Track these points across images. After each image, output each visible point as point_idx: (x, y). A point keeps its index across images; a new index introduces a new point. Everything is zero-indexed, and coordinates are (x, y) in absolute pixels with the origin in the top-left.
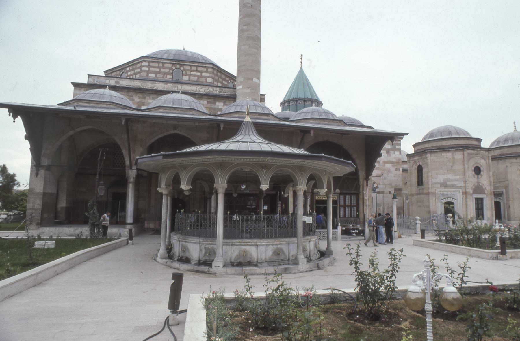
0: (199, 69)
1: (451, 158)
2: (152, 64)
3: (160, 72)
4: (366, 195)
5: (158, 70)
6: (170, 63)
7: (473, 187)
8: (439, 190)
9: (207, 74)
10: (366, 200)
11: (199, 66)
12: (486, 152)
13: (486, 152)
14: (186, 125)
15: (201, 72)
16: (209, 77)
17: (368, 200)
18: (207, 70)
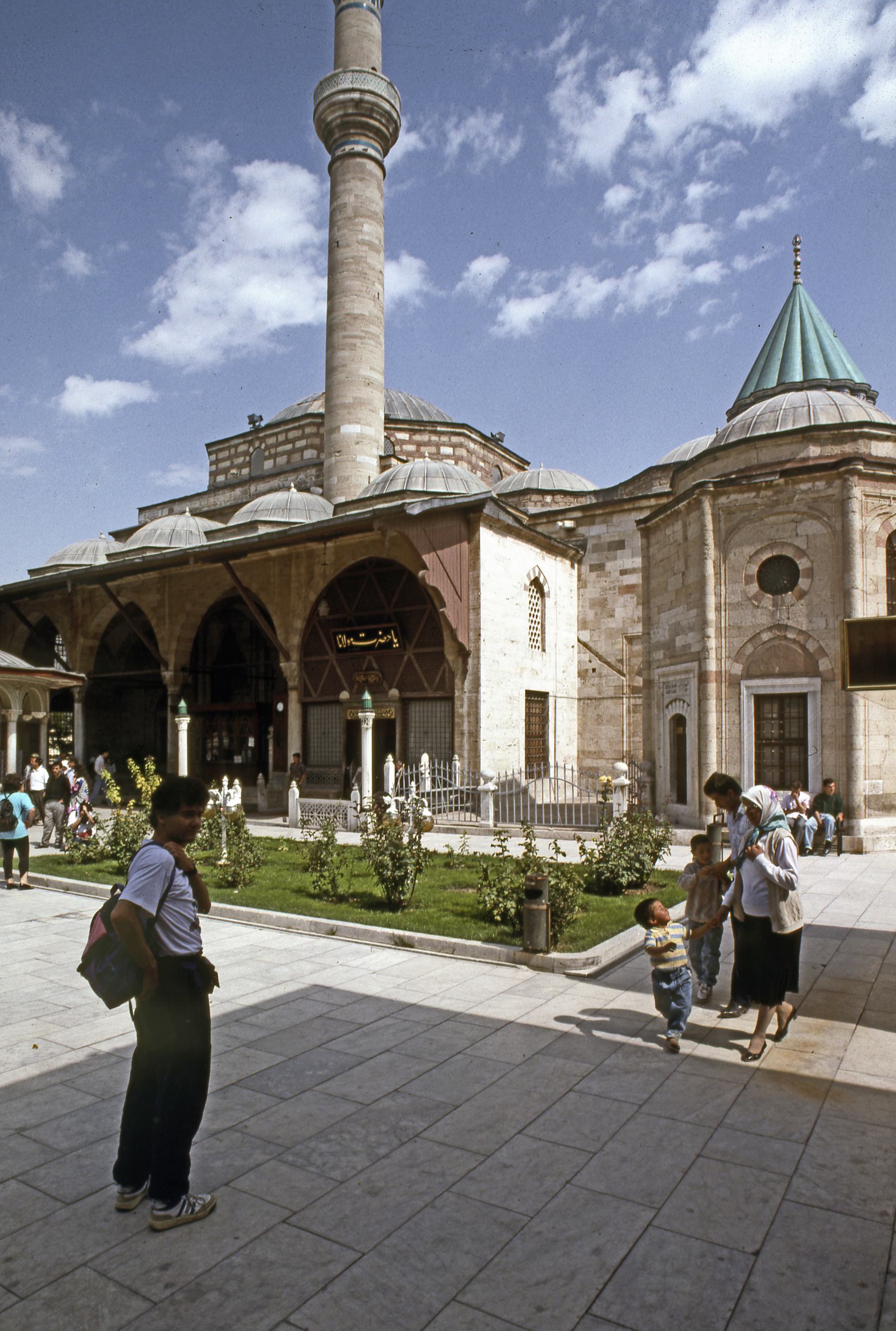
0: (291, 435)
1: (682, 542)
2: (221, 455)
3: (232, 466)
4: (462, 700)
5: (227, 464)
6: (244, 443)
7: (750, 649)
8: (660, 671)
9: (301, 443)
10: (462, 716)
11: (290, 430)
12: (829, 485)
13: (829, 485)
14: (130, 584)
15: (293, 441)
16: (306, 447)
17: (469, 714)
18: (303, 432)
